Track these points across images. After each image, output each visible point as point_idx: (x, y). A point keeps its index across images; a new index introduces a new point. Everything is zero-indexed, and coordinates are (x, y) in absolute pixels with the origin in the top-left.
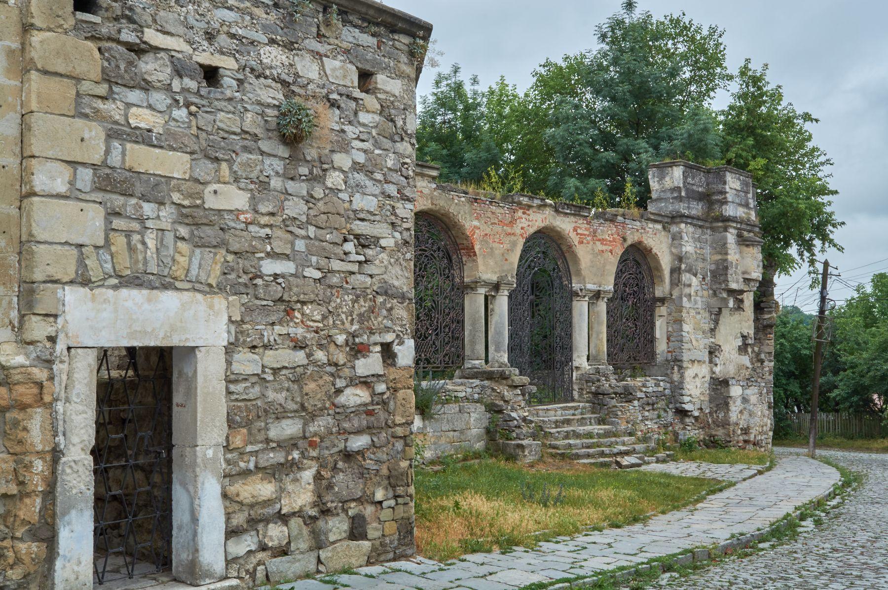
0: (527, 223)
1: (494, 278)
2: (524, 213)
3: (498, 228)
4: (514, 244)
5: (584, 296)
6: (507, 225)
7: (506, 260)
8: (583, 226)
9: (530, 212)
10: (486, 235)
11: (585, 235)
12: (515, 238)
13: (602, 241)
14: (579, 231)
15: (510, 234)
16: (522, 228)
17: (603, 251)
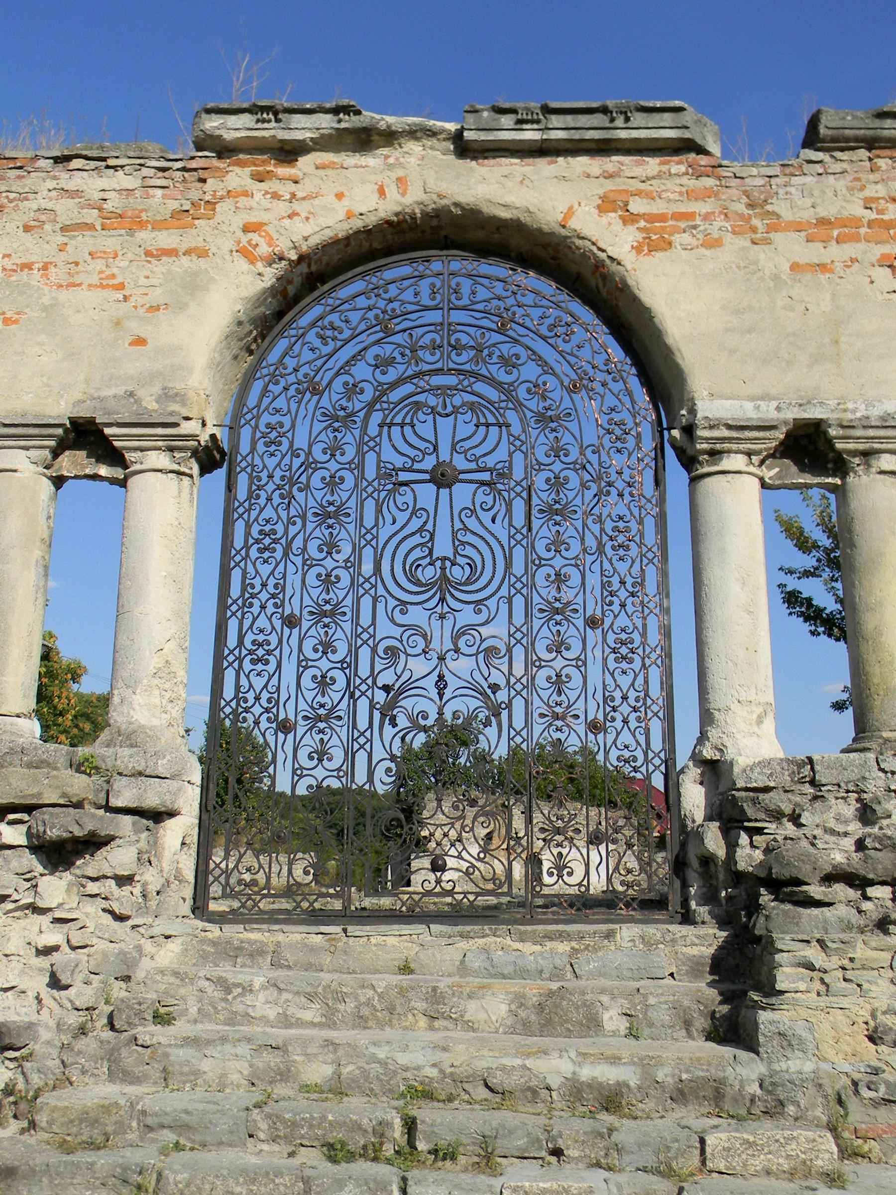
0: (282, 208)
1: (61, 409)
2: (259, 178)
3: (110, 242)
4: (194, 286)
5: (715, 454)
6: (158, 226)
7: (140, 341)
8: (671, 184)
9: (305, 162)
10: (28, 266)
11: (691, 216)
12: (202, 263)
13: (822, 228)
14: (637, 206)
15: (171, 252)
16: (246, 229)
17: (823, 267)
